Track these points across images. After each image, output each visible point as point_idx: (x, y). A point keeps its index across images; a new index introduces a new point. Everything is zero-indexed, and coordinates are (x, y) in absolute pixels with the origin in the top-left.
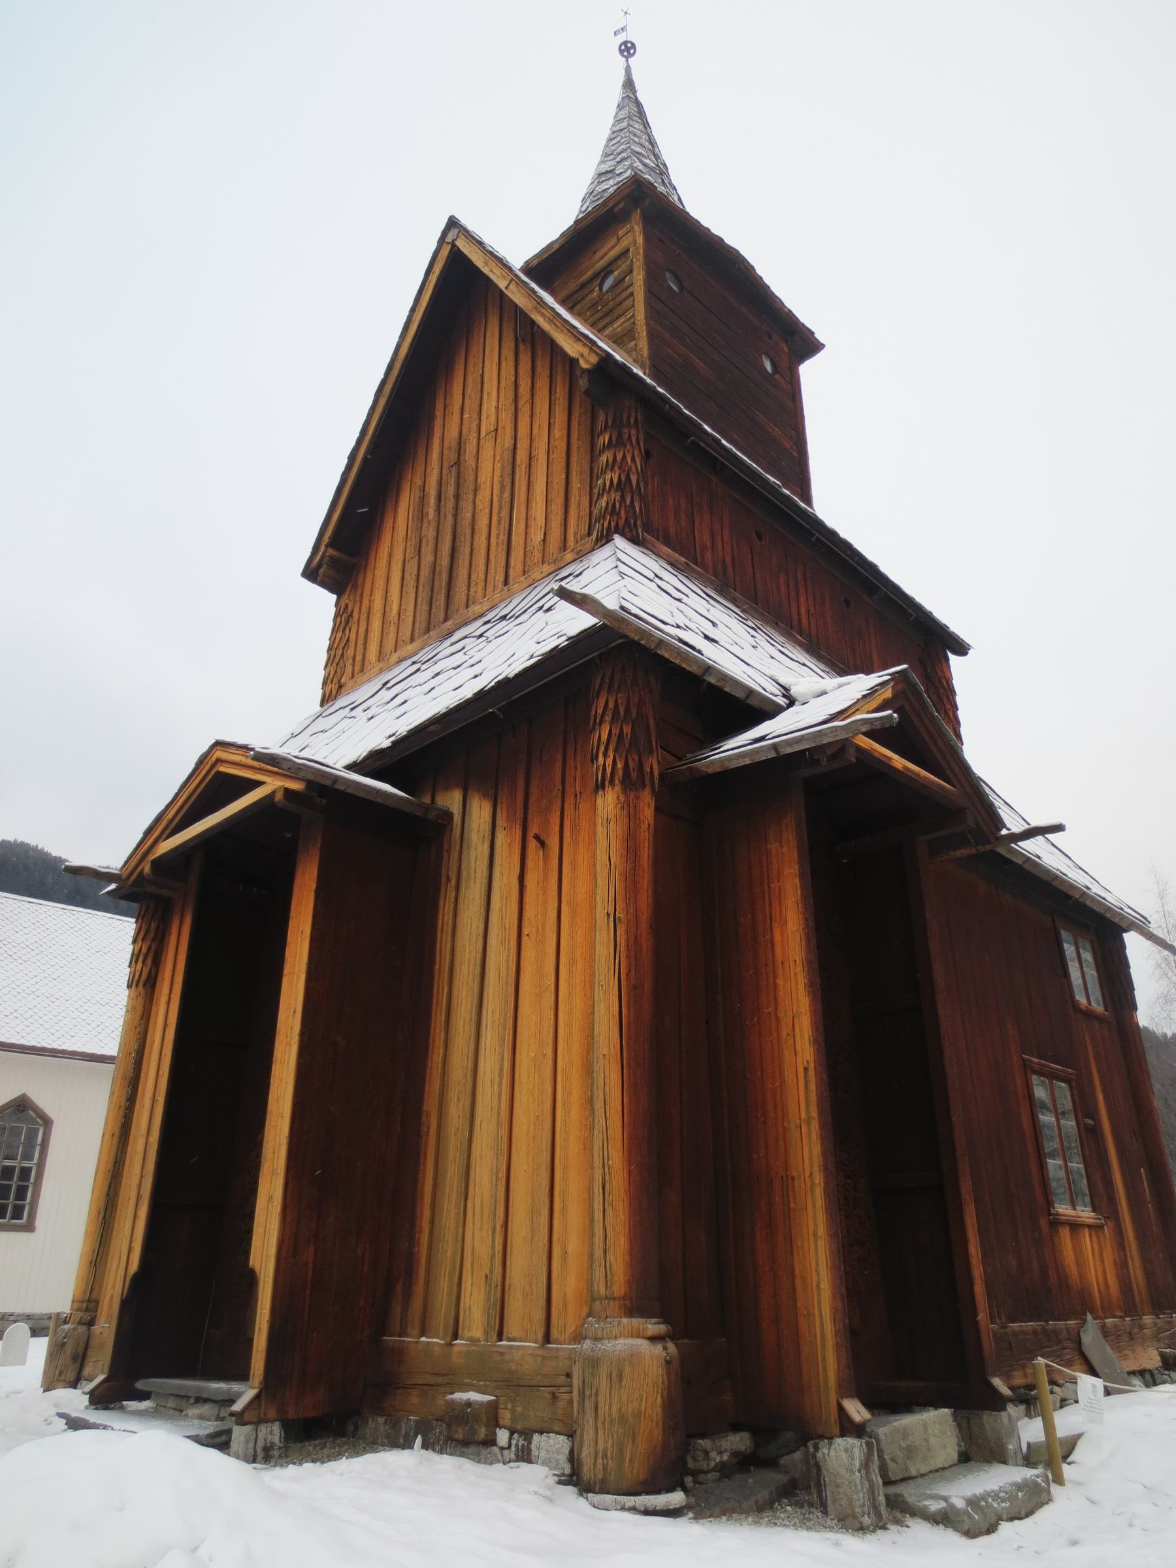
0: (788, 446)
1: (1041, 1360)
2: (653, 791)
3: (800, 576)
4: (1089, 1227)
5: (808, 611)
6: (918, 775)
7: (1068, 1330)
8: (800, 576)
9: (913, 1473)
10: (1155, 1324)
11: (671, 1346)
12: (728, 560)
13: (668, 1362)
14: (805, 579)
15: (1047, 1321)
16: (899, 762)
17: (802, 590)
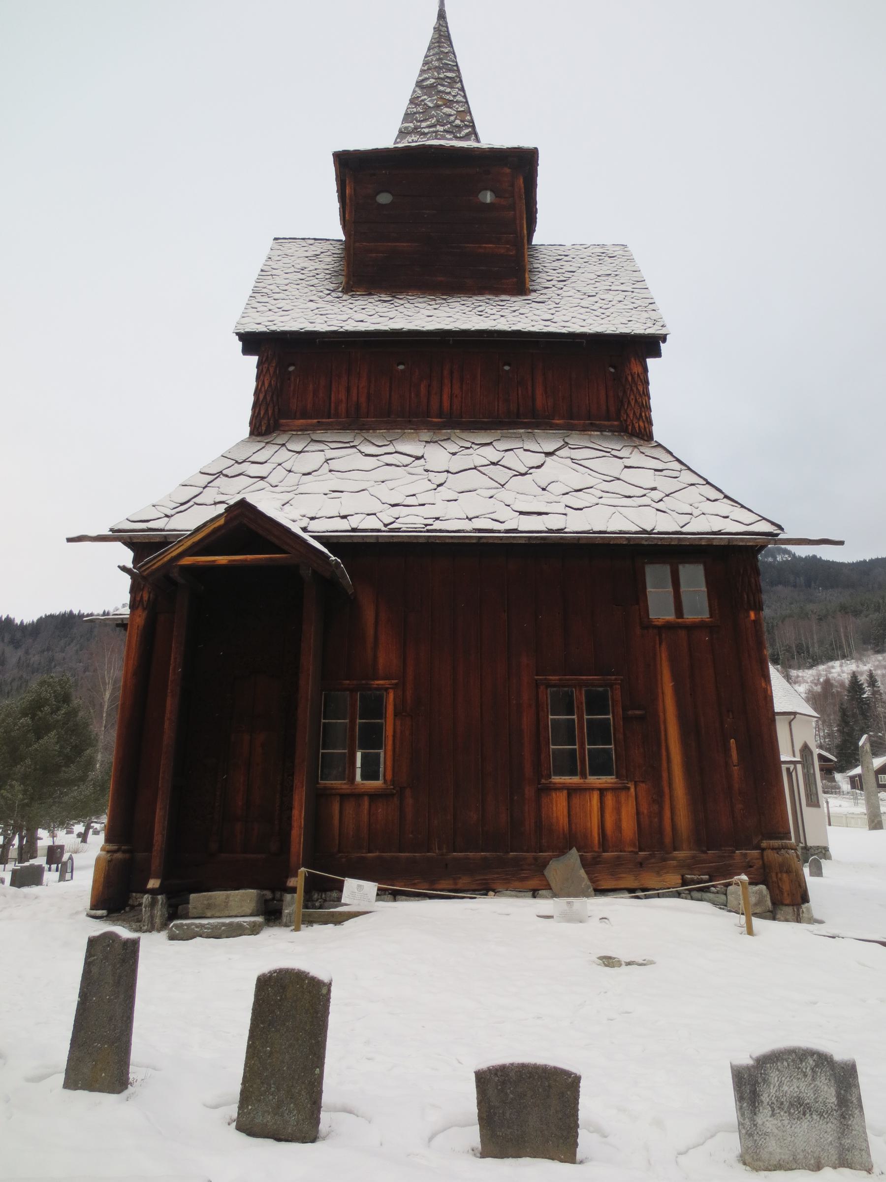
0: (502, 251)
1: (303, 869)
2: (144, 609)
3: (446, 372)
4: (613, 789)
5: (451, 397)
6: (246, 560)
7: (536, 859)
8: (446, 372)
9: (209, 915)
10: (693, 857)
11: (119, 855)
12: (363, 399)
13: (110, 861)
14: (452, 373)
15: (508, 853)
16: (222, 560)
17: (447, 381)
